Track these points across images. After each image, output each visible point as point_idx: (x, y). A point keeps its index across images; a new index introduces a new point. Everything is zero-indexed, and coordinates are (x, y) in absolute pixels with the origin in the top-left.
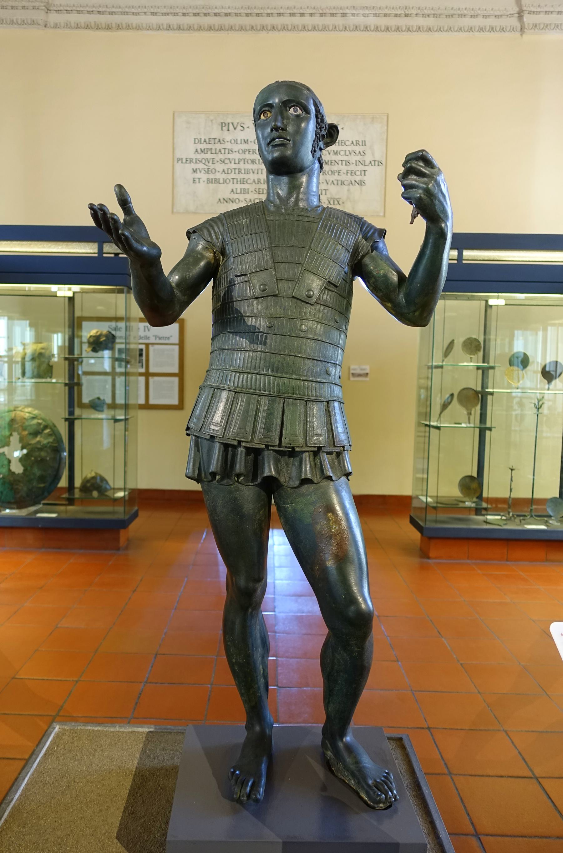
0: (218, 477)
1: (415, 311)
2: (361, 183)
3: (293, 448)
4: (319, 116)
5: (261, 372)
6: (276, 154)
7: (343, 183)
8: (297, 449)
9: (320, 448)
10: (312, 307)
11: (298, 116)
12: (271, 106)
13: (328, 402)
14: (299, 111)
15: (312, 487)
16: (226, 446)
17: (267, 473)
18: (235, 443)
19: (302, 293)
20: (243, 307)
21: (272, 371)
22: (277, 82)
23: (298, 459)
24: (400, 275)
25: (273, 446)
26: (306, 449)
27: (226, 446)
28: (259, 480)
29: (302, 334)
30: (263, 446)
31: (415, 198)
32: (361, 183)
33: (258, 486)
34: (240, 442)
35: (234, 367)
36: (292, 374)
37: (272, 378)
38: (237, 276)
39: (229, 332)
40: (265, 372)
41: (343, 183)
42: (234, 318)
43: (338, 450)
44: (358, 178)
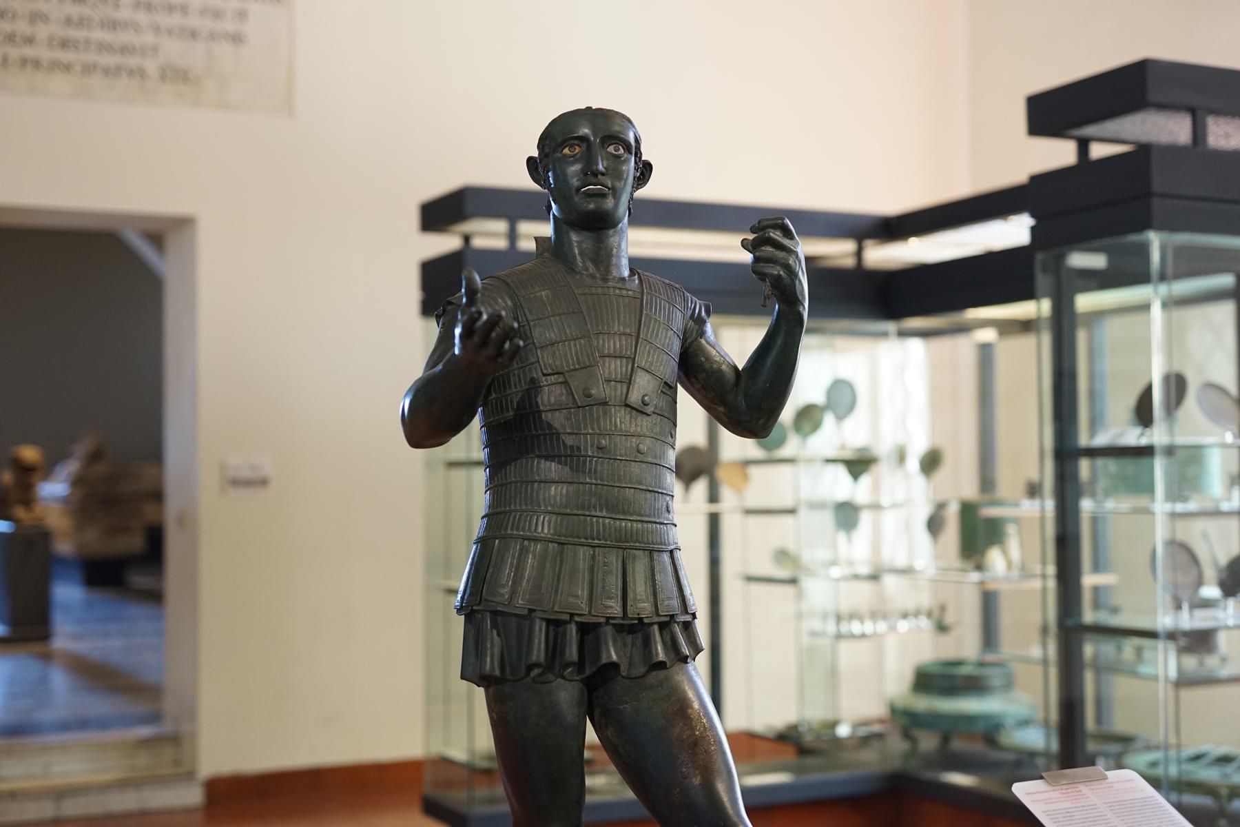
0: (536, 671)
1: (758, 419)
2: (237, 39)
3: (641, 619)
4: (638, 154)
5: (593, 513)
6: (592, 206)
7: (194, 35)
8: (646, 621)
9: (672, 616)
10: (649, 419)
11: (618, 157)
12: (583, 139)
13: (671, 552)
14: (622, 151)
15: (661, 674)
16: (549, 622)
17: (604, 660)
18: (566, 617)
19: (635, 397)
20: (557, 420)
21: (608, 510)
22: (589, 108)
23: (640, 635)
24: (735, 368)
25: (614, 618)
26: (656, 619)
27: (549, 622)
28: (588, 672)
29: (641, 457)
30: (602, 620)
31: (772, 275)
32: (237, 39)
33: (581, 681)
34: (572, 615)
35: (553, 506)
36: (632, 514)
37: (607, 521)
38: (544, 375)
39: (539, 457)
40: (598, 514)
41: (194, 35)
42: (545, 435)
43: (688, 618)
44: (229, 26)
